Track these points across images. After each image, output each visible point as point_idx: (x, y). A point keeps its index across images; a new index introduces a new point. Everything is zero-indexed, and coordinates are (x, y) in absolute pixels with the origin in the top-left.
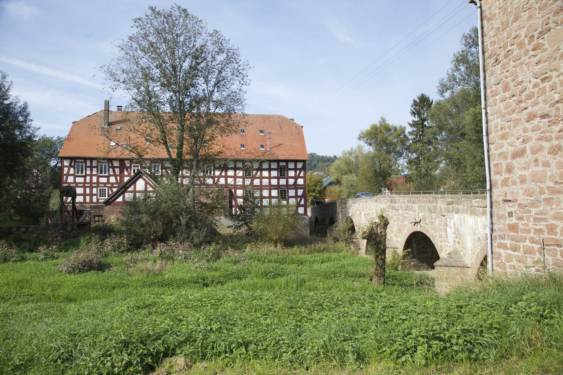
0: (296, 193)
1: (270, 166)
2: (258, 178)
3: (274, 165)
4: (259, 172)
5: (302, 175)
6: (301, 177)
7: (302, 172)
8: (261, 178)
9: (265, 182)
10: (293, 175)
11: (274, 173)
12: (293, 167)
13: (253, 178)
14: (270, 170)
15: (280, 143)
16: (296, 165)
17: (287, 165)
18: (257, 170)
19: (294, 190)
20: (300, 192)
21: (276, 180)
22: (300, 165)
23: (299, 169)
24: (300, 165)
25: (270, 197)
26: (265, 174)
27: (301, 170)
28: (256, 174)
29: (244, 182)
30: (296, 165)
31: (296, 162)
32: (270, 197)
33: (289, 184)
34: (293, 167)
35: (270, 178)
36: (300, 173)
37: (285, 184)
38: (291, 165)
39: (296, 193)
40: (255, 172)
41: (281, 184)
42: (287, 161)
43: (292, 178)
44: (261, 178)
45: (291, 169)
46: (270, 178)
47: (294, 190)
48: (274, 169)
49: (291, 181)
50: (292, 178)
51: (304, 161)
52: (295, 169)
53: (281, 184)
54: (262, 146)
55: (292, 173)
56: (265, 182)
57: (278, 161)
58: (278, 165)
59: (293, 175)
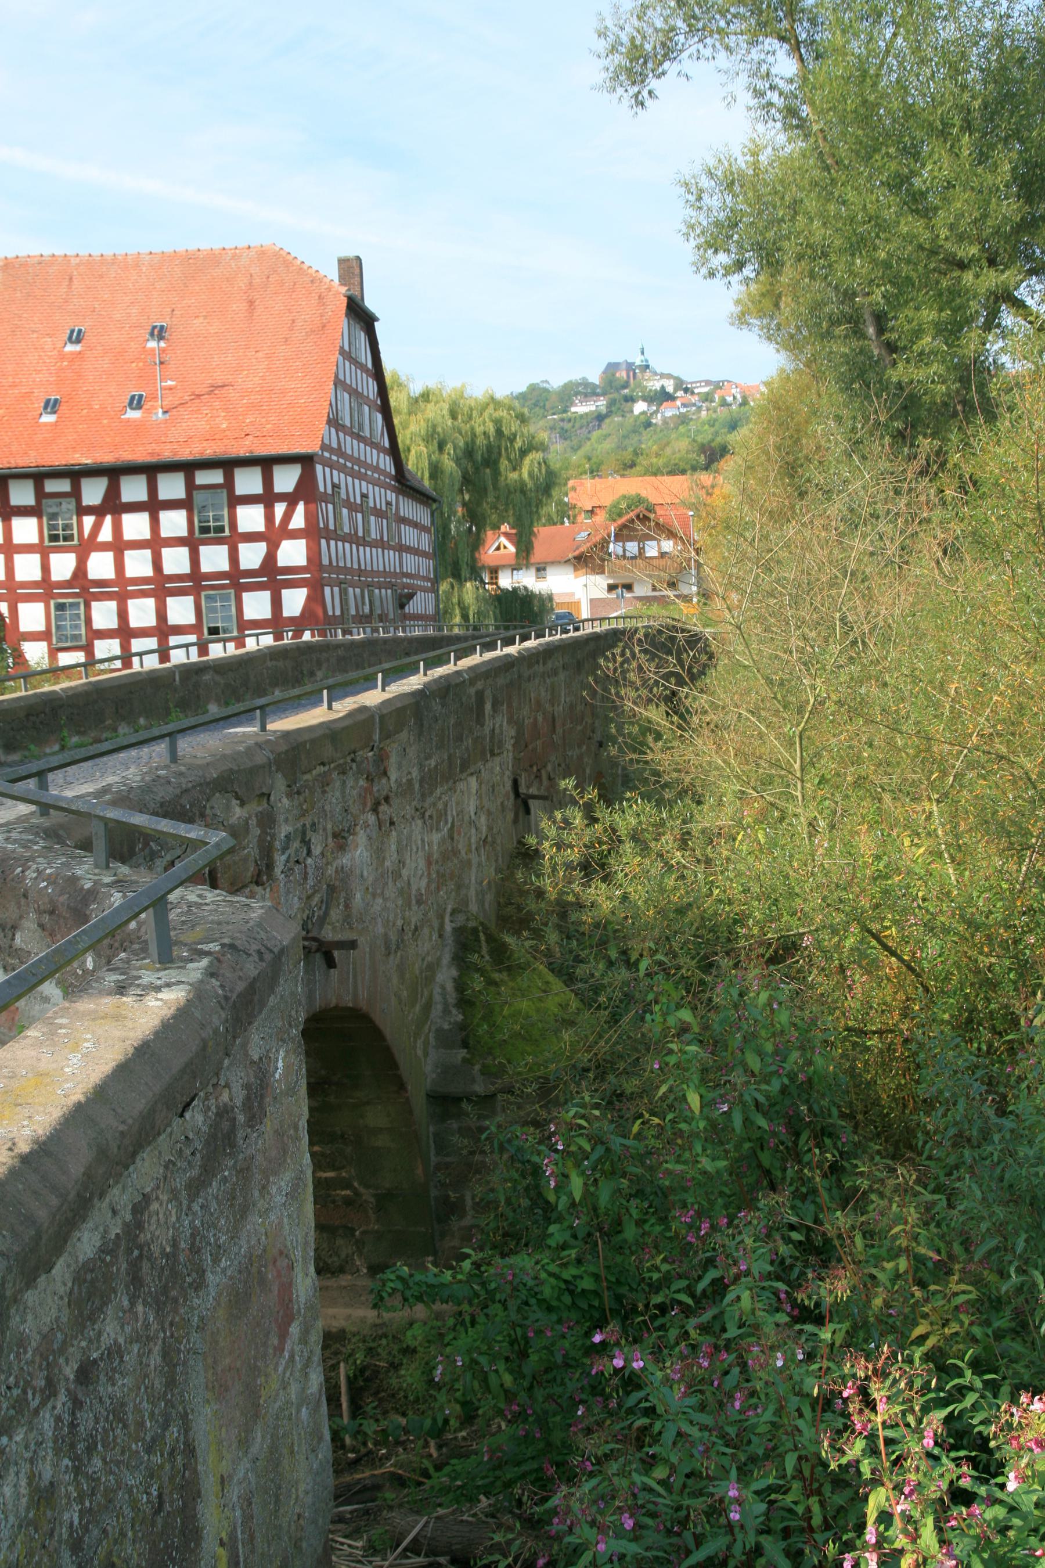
0: (277, 603)
1: (153, 489)
2: (104, 547)
3: (172, 487)
4: (108, 519)
5: (298, 521)
6: (294, 535)
7: (301, 507)
8: (119, 546)
9: (139, 564)
10: (260, 526)
11: (174, 523)
12: (258, 489)
13: (85, 549)
14: (153, 506)
15: (219, 378)
16: (268, 481)
17: (229, 483)
18: (99, 512)
19: (267, 594)
20: (294, 601)
21: (184, 552)
22: (286, 480)
23: (282, 497)
24: (286, 480)
25: (163, 630)
26: (136, 526)
27: (291, 500)
28: (97, 528)
29: (46, 568)
30: (268, 481)
31: (267, 464)
32: (163, 630)
33: (243, 567)
34: (258, 489)
35: (156, 544)
36: (288, 516)
37: (225, 566)
38: (248, 482)
39: (277, 603)
40: (89, 521)
41: (205, 567)
42: (229, 465)
43: (252, 537)
44: (119, 546)
45: (249, 500)
46: (156, 544)
47: (267, 594)
48: (172, 505)
49: (252, 556)
50: (252, 537)
51: (306, 461)
52: (268, 498)
53: (205, 567)
54: (136, 403)
55: (251, 518)
56: (139, 564)
57: (188, 468)
58: (191, 486)
59: (260, 526)
